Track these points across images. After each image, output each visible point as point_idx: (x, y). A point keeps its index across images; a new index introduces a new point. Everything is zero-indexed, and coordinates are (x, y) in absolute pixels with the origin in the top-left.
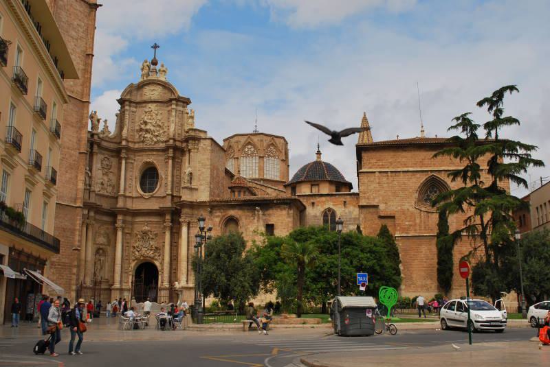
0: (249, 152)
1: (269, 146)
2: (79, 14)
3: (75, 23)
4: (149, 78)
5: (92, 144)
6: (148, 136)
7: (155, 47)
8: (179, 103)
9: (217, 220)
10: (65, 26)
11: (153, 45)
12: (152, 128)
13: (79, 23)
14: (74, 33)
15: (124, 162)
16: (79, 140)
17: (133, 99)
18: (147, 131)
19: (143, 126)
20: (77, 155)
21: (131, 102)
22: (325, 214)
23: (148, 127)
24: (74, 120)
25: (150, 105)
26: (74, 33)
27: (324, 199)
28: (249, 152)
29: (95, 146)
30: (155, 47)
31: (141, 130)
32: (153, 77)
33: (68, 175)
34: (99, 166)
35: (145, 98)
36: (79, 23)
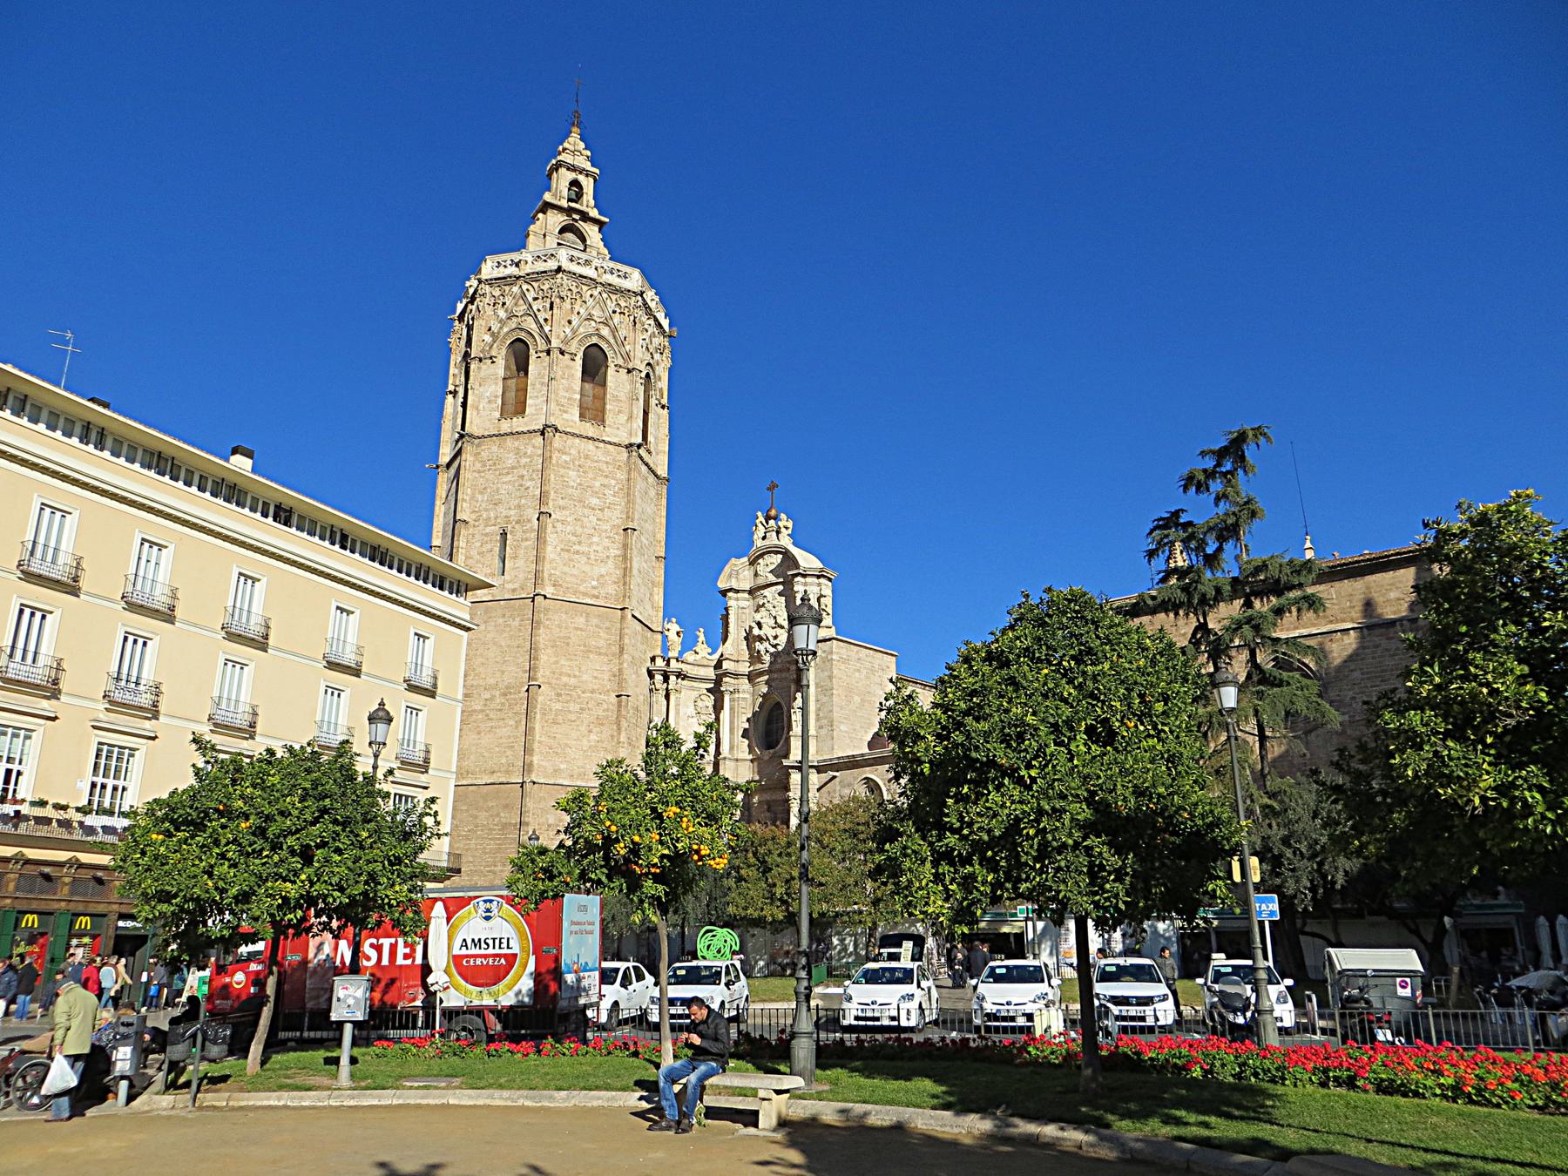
2: (604, 467)
3: (597, 484)
4: (767, 542)
5: (666, 679)
7: (772, 487)
8: (809, 580)
10: (576, 493)
11: (768, 484)
12: (770, 633)
13: (606, 481)
14: (594, 501)
15: (727, 698)
16: (619, 676)
18: (760, 639)
19: (756, 631)
20: (614, 700)
21: (737, 591)
23: (762, 633)
24: (602, 643)
25: (766, 592)
26: (594, 501)
29: (673, 678)
30: (772, 487)
33: (593, 737)
34: (691, 710)
35: (761, 581)
36: (606, 481)
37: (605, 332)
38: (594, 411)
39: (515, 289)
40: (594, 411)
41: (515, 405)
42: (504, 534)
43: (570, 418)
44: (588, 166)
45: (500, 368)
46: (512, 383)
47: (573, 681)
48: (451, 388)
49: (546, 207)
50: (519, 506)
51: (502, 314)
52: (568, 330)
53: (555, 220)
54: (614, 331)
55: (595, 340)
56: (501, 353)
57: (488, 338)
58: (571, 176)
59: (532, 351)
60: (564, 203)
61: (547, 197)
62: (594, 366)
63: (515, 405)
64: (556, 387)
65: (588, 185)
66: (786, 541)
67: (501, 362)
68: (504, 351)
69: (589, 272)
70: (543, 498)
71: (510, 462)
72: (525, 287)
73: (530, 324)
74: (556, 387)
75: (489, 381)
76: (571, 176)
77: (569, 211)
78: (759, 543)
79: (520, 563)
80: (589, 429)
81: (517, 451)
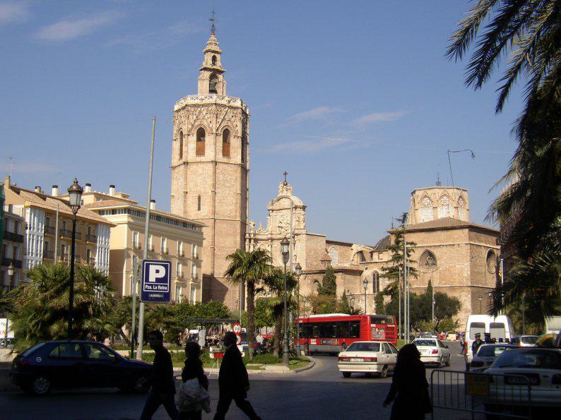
0: (426, 204)
1: (442, 197)
6: (283, 230)
7: (286, 174)
9: (309, 281)
13: (230, 177)
14: (228, 185)
17: (274, 208)
19: (280, 225)
22: (374, 275)
26: (228, 185)
27: (372, 265)
28: (426, 204)
29: (252, 240)
30: (286, 174)
31: (279, 227)
32: (285, 193)
37: (229, 124)
38: (226, 152)
39: (199, 109)
40: (226, 152)
41: (200, 151)
42: (199, 198)
43: (220, 157)
44: (217, 49)
45: (195, 138)
46: (200, 143)
47: (223, 245)
48: (174, 138)
49: (205, 69)
50: (204, 188)
51: (195, 118)
52: (218, 125)
53: (207, 74)
54: (232, 123)
55: (226, 127)
56: (195, 132)
57: (190, 126)
58: (213, 54)
59: (206, 133)
60: (210, 67)
61: (204, 65)
62: (226, 134)
63: (200, 151)
64: (212, 145)
65: (218, 56)
66: (289, 194)
67: (195, 136)
68: (195, 133)
69: (224, 102)
70: (214, 185)
71: (201, 172)
72: (202, 109)
73: (205, 123)
74: (212, 145)
75: (191, 142)
76: (213, 54)
77: (214, 69)
78: (281, 194)
79: (206, 206)
80: (225, 160)
81: (203, 169)
